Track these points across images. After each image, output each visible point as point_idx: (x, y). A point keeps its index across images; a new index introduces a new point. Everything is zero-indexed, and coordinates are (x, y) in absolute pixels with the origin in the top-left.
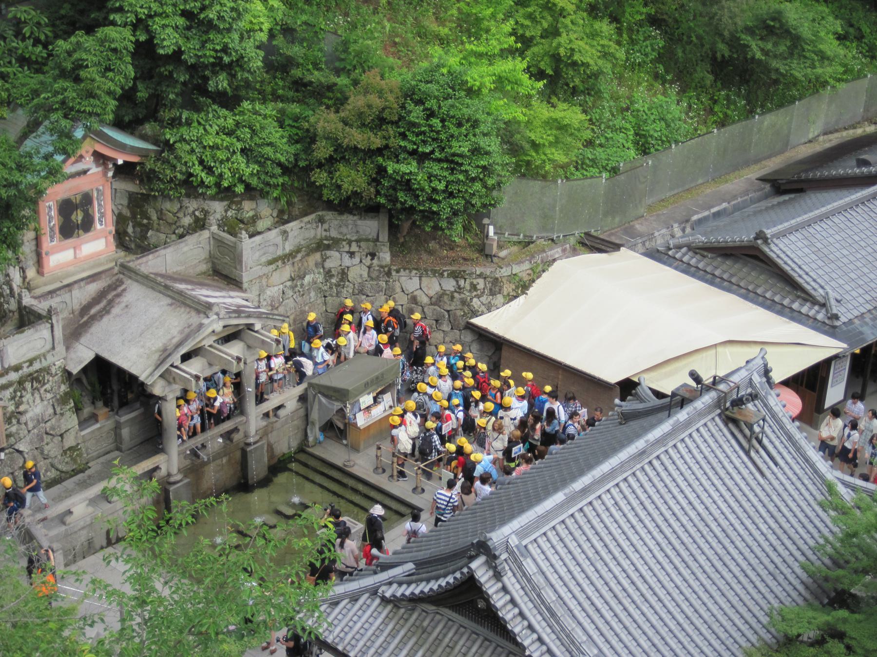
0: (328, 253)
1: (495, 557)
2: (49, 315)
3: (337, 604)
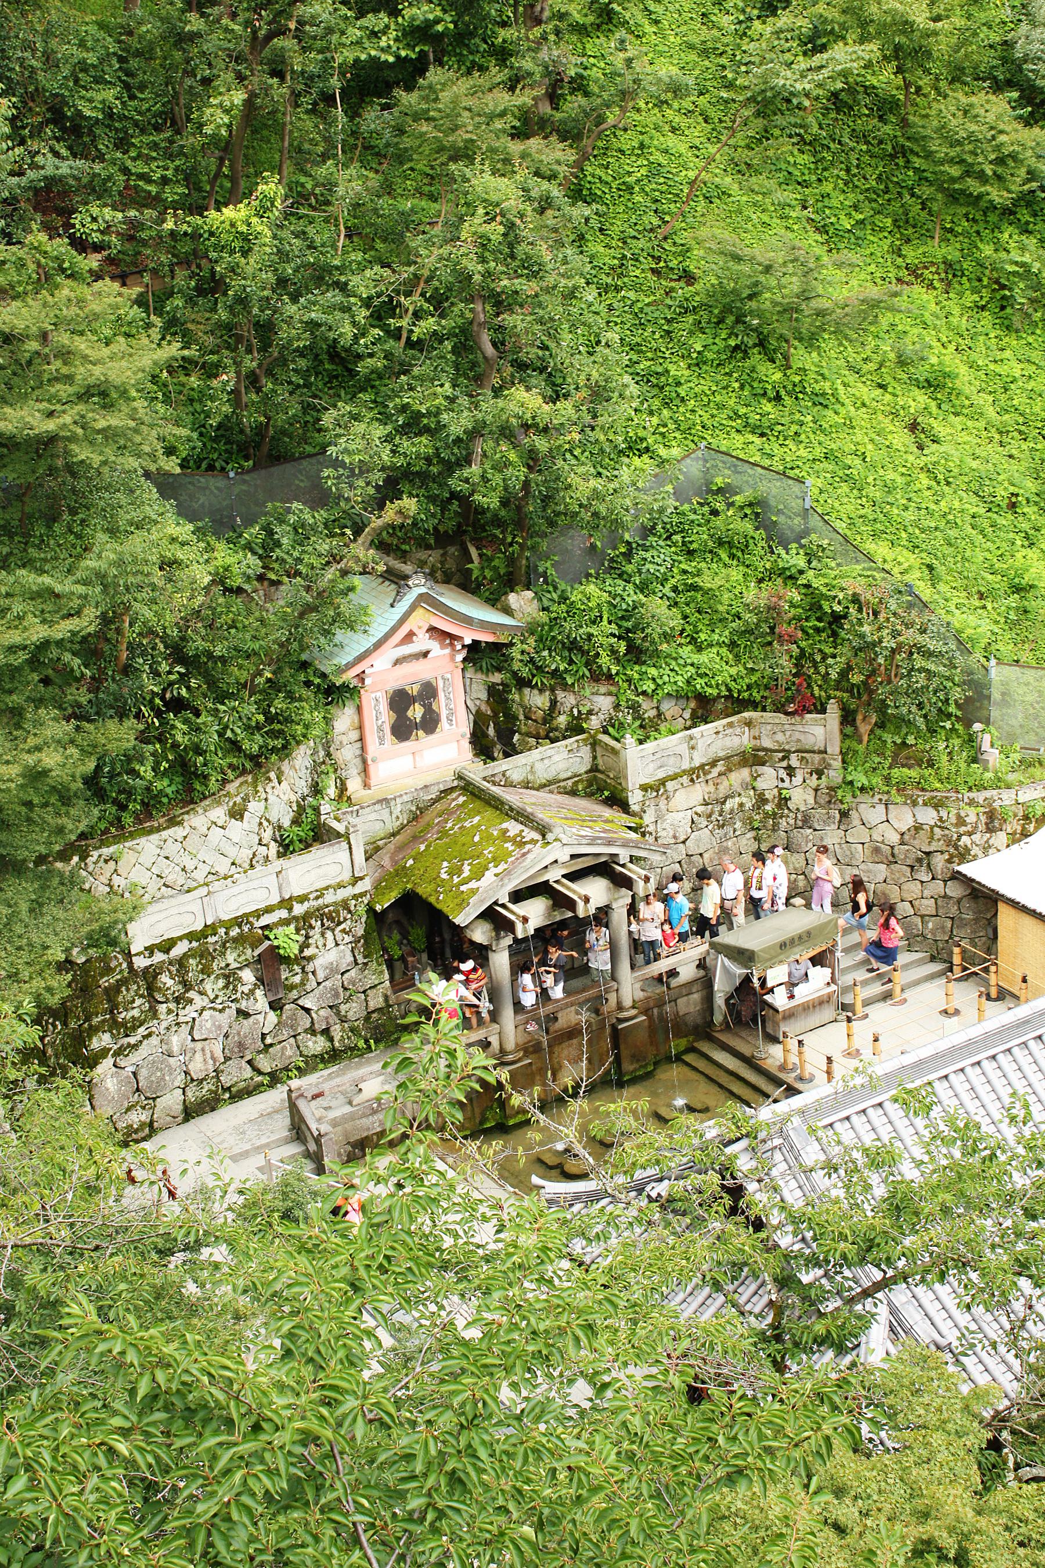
0: (761, 769)
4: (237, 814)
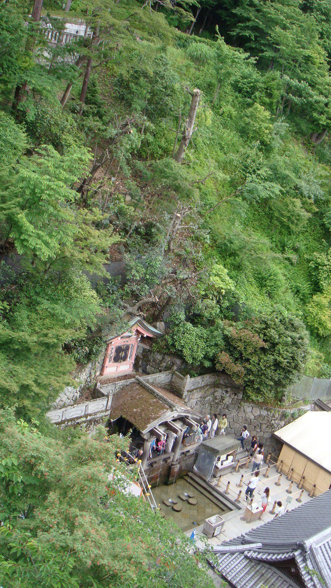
0: (217, 389)
1: (306, 552)
2: (108, 396)
3: (225, 554)
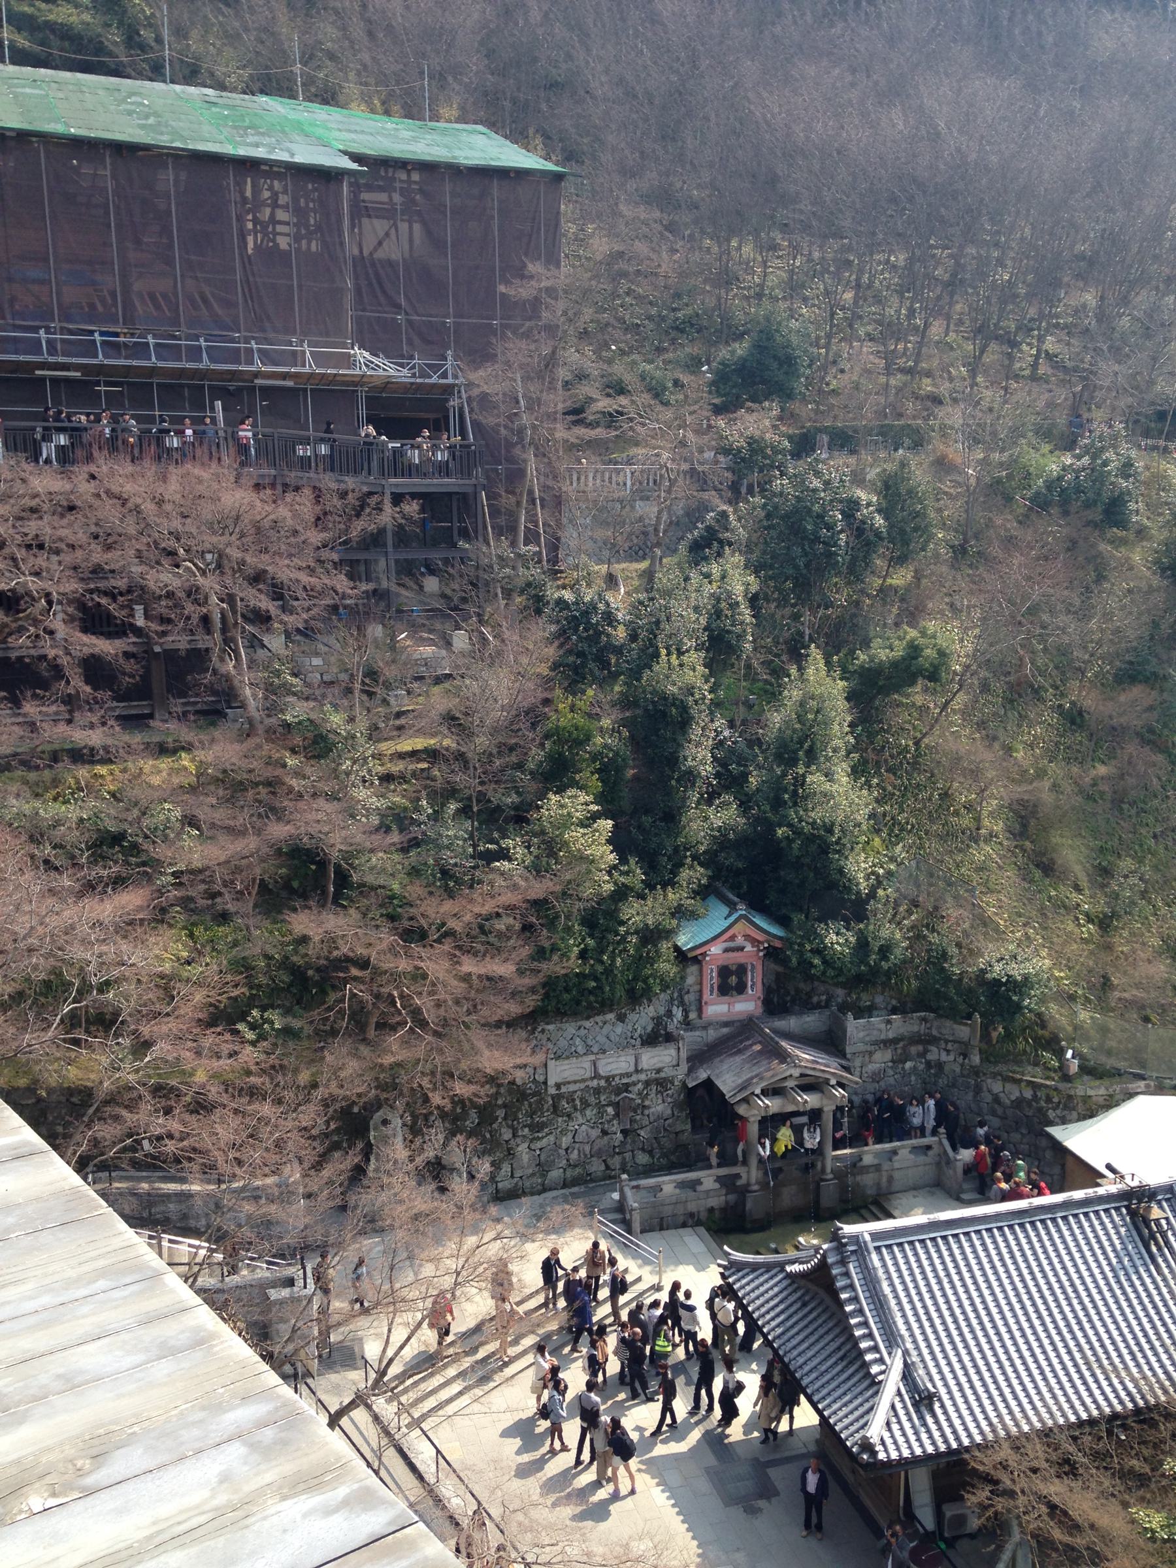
4: (621, 1018)
